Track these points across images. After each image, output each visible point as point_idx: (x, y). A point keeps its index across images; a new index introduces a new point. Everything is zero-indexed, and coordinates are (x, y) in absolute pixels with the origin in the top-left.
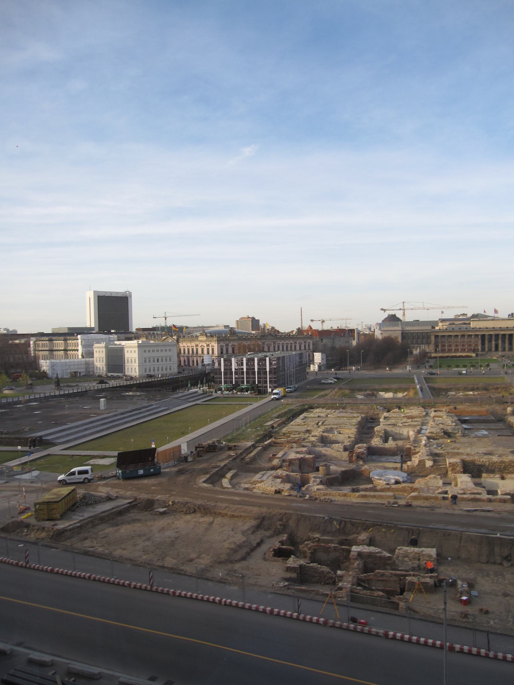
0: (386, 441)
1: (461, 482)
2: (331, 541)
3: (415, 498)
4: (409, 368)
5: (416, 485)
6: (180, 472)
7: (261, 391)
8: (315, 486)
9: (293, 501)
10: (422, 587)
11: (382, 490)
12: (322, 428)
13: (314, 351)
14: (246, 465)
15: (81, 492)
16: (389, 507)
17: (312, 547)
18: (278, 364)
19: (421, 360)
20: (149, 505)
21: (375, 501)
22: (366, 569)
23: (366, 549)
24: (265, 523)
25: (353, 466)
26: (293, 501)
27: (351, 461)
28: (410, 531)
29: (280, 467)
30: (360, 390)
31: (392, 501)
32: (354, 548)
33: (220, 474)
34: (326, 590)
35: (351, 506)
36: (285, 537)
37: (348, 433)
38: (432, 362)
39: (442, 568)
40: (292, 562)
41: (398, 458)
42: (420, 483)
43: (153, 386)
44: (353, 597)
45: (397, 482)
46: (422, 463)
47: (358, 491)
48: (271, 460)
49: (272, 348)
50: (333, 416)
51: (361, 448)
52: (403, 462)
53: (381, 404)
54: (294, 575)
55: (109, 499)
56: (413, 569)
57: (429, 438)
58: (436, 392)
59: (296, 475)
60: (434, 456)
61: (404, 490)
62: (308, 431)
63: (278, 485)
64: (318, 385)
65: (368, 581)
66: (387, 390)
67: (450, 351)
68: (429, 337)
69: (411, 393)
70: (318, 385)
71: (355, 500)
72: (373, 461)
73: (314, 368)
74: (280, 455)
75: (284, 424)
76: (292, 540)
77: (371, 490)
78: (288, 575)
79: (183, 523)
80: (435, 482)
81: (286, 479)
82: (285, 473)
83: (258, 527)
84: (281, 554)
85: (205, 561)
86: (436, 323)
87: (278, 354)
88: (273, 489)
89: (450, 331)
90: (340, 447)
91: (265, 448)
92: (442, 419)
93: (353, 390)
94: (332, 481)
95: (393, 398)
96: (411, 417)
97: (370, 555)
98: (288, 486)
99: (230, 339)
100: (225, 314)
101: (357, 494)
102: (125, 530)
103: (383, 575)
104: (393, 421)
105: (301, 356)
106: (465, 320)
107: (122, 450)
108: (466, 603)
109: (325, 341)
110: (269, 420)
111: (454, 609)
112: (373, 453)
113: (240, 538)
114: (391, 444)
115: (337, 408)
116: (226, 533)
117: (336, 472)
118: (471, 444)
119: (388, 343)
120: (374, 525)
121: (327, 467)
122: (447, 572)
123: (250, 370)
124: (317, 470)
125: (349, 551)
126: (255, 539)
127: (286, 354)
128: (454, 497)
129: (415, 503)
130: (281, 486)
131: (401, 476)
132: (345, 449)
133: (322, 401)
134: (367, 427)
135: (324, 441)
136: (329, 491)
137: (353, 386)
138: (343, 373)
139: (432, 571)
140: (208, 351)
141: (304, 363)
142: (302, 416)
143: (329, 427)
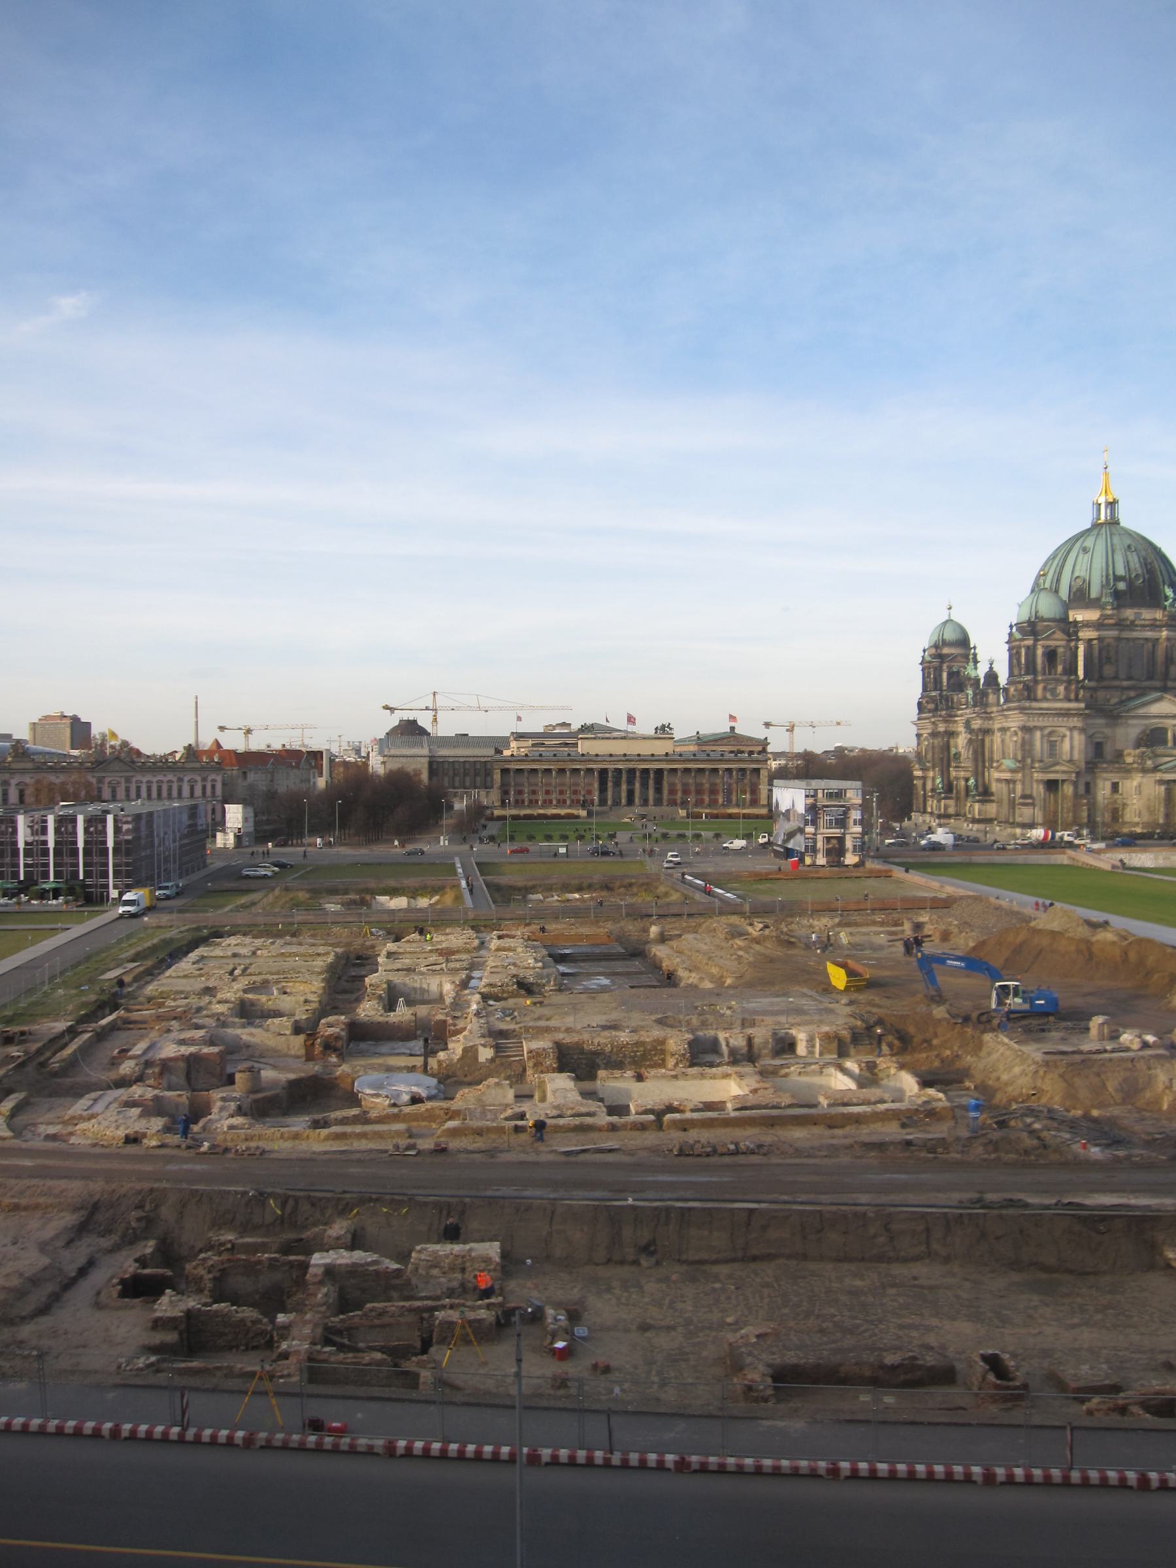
0: (391, 1006)
1: (554, 1092)
2: (263, 1247)
3: (454, 1133)
4: (444, 841)
5: (457, 1104)
8: (224, 1120)
9: (170, 1159)
10: (469, 1330)
11: (381, 1120)
12: (243, 982)
13: (227, 800)
16: (397, 1158)
17: (213, 1266)
18: (136, 830)
19: (472, 825)
21: (364, 1145)
22: (344, 1304)
23: (343, 1258)
24: (100, 1217)
25: (315, 1068)
26: (170, 1159)
27: (309, 1057)
28: (443, 1208)
29: (140, 1079)
30: (333, 891)
31: (403, 1142)
32: (319, 1259)
34: (250, 1363)
35: (308, 1161)
36: (149, 1247)
37: (303, 992)
38: (493, 829)
39: (512, 1285)
40: (168, 1305)
41: (417, 1045)
42: (465, 1098)
44: (315, 1372)
45: (415, 1100)
46: (470, 1053)
47: (326, 1124)
48: (114, 1063)
49: (121, 793)
50: (267, 954)
51: (333, 1026)
52: (429, 1053)
53: (379, 924)
54: (171, 1337)
56: (451, 1293)
57: (485, 997)
58: (502, 894)
59: (179, 1097)
60: (497, 1036)
61: (430, 1116)
62: (209, 991)
63: (134, 1122)
64: (233, 880)
65: (349, 1331)
66: (393, 892)
67: (533, 803)
68: (489, 773)
69: (449, 899)
70: (233, 880)
71: (318, 1147)
72: (362, 1054)
73: (225, 840)
74: (138, 1050)
75: (150, 974)
76: (168, 1254)
77: (355, 1120)
78: (158, 1338)
80: (498, 1094)
81: (155, 1108)
82: (150, 1093)
84: (139, 1288)
86: (503, 742)
87: (138, 806)
88: (121, 1133)
89: (533, 761)
90: (284, 1024)
91: (101, 1036)
92: (513, 954)
93: (316, 893)
94: (264, 1107)
95: (409, 910)
96: (447, 953)
97: (354, 1271)
98: (157, 1123)
101: (324, 1132)
103: (382, 1314)
104: (407, 962)
105: (193, 811)
106: (566, 737)
108: (563, 1355)
109: (251, 777)
110: (112, 966)
111: (539, 1370)
112: (363, 1036)
114: (402, 1014)
115: (280, 935)
117: (274, 1084)
118: (575, 1008)
119: (398, 785)
120: (363, 1201)
121: (254, 1072)
122: (525, 1292)
124: (231, 1080)
125: (304, 1267)
127: (157, 806)
128: (540, 1126)
129: (454, 1144)
130: (139, 1126)
131: (423, 1085)
132: (297, 1029)
133: (241, 918)
134: (346, 977)
135: (247, 1012)
136: (259, 1129)
137: (321, 882)
138: (291, 853)
139: (487, 1293)
142: (193, 956)
143: (256, 978)
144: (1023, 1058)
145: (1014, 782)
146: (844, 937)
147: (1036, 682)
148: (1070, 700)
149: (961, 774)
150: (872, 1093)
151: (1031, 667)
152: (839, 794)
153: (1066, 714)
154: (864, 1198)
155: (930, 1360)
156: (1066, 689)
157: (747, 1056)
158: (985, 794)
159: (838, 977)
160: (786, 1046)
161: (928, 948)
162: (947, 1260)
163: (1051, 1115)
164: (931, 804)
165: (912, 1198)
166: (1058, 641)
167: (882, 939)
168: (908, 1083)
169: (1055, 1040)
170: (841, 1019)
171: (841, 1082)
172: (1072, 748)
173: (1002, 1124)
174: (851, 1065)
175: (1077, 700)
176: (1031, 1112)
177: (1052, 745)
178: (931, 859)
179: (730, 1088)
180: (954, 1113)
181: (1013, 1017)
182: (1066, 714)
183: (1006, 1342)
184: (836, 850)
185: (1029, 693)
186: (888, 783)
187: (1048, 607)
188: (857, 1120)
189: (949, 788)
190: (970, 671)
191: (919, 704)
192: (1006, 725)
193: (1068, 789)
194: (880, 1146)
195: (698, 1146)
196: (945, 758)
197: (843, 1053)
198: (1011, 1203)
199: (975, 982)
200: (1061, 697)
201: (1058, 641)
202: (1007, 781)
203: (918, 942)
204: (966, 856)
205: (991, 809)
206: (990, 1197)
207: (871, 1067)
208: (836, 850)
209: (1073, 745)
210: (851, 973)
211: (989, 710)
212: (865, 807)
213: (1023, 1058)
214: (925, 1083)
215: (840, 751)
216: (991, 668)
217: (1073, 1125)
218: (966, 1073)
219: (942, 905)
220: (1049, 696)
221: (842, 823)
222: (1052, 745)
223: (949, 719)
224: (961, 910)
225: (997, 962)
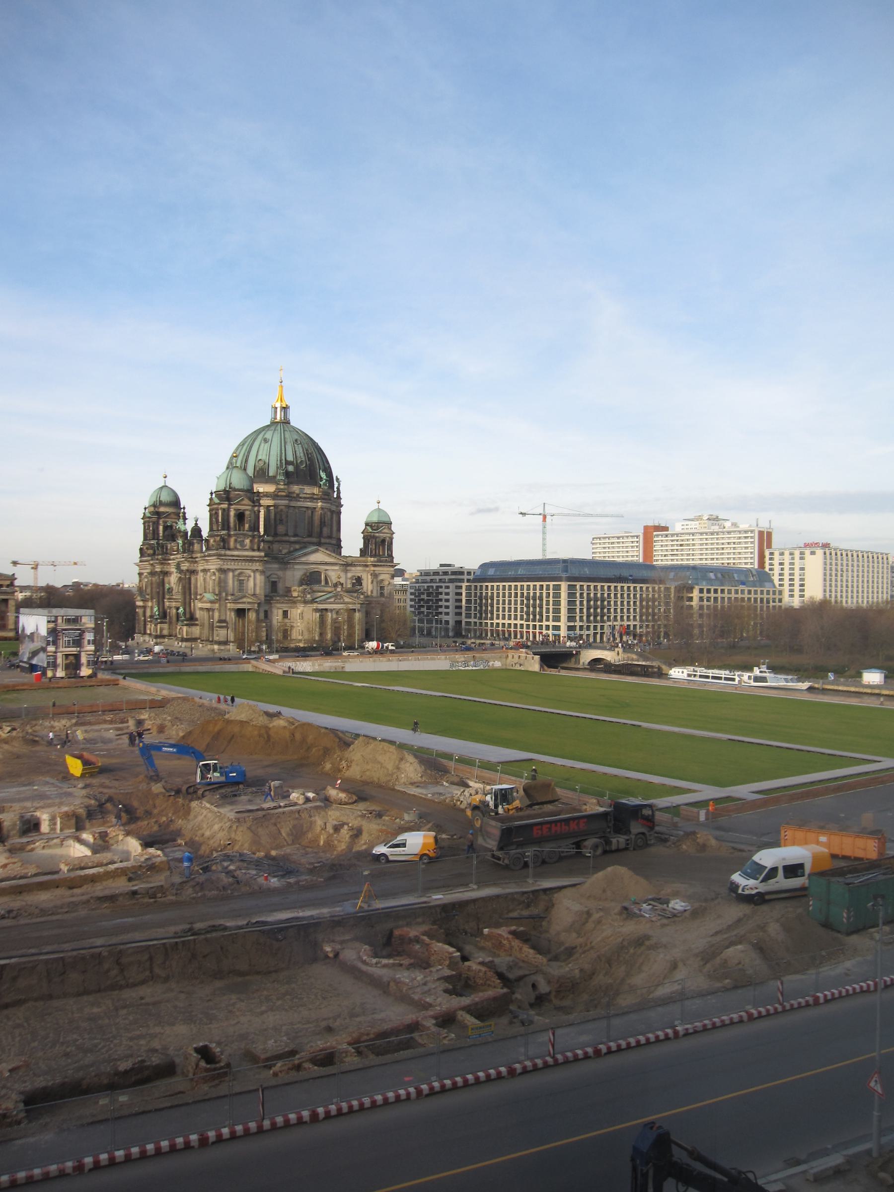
144: (221, 817)
145: (213, 610)
146: (80, 734)
147: (229, 536)
148: (253, 550)
149: (173, 604)
150: (105, 856)
151: (226, 525)
152: (76, 620)
153: (251, 560)
154: (99, 942)
155: (155, 1060)
156: (251, 541)
158: (191, 619)
159: (75, 767)
161: (148, 739)
162: (166, 979)
163: (242, 858)
164: (150, 628)
165: (137, 936)
166: (245, 506)
167: (111, 734)
168: (133, 845)
169: (245, 802)
170: (78, 799)
171: (78, 851)
172: (255, 585)
173: (206, 869)
174: (87, 836)
175: (259, 550)
176: (228, 858)
177: (241, 582)
180: (169, 866)
181: (215, 787)
182: (251, 560)
185: (224, 544)
186: (116, 611)
187: (238, 481)
188: (93, 879)
189: (164, 615)
190: (180, 525)
191: (141, 549)
192: (207, 567)
193: (252, 616)
194: (112, 898)
196: (161, 592)
197: (80, 827)
198: (214, 928)
199: (185, 763)
200: (247, 547)
201: (245, 506)
202: (208, 610)
203: (140, 735)
204: (173, 667)
205: (196, 631)
206: (198, 926)
207: (103, 836)
209: (256, 583)
210: (86, 763)
211: (194, 556)
212: (97, 630)
213: (221, 817)
214: (146, 844)
215: (77, 585)
216: (196, 524)
217: (258, 864)
218: (178, 833)
219: (158, 705)
220: (239, 546)
221: (78, 643)
222: (241, 582)
223: (164, 562)
224: (170, 708)
225: (201, 746)
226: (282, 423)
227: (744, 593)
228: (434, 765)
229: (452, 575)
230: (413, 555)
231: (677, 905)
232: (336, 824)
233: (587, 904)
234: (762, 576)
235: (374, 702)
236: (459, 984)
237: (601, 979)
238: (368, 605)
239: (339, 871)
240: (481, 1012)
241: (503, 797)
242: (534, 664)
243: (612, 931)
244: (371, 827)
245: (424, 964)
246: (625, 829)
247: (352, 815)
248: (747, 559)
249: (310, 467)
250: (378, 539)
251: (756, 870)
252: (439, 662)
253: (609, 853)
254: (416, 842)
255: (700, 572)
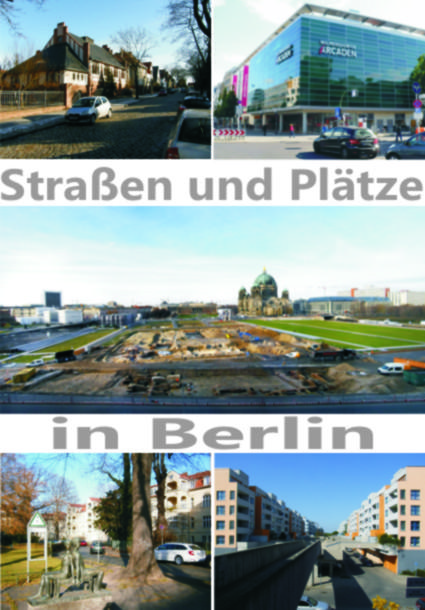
6: (85, 358)
7: (117, 327)
8: (138, 358)
14: (112, 353)
15: (38, 369)
19: (174, 316)
20: (70, 372)
33: (102, 357)
34: (143, 393)
40: (131, 385)
42: (175, 354)
43: (72, 327)
44: (153, 394)
51: (154, 345)
55: (52, 371)
79: (86, 377)
81: (128, 357)
83: (116, 376)
84: (126, 383)
85: (96, 389)
92: (181, 334)
94: (144, 356)
99: (105, 310)
100: (105, 300)
102: (60, 382)
106: (188, 304)
107: (58, 351)
111: (186, 392)
112: (159, 346)
113: (109, 379)
114: (165, 343)
116: (104, 378)
119: (163, 311)
122: (184, 381)
123: (113, 320)
126: (116, 379)
134: (156, 338)
135: (142, 343)
137: (152, 324)
140: (96, 314)
141: (133, 317)
143: (143, 338)
149: (245, 308)
157: (215, 347)
160: (220, 346)
169: (259, 344)
170: (228, 342)
178: (241, 320)
179: (213, 352)
183: (253, 386)
184: (227, 318)
186: (235, 309)
187: (256, 285)
195: (208, 360)
204: (246, 319)
208: (227, 318)
209: (260, 303)
219: (242, 326)
226: (265, 273)
227: (381, 303)
228: (299, 339)
229: (303, 301)
230: (294, 297)
231: (362, 373)
232: (278, 349)
233: (334, 370)
234: (387, 298)
235: (286, 326)
236: (305, 383)
237: (342, 387)
238: (283, 307)
239: (278, 358)
240: (312, 390)
241: (316, 346)
242: (322, 319)
243: (344, 377)
244: (285, 351)
245: (297, 378)
246: (347, 355)
247: (281, 348)
248: (382, 295)
249: (271, 281)
250: (285, 295)
251: (386, 368)
252: (299, 318)
253: (342, 360)
254: (295, 354)
255: (368, 299)
